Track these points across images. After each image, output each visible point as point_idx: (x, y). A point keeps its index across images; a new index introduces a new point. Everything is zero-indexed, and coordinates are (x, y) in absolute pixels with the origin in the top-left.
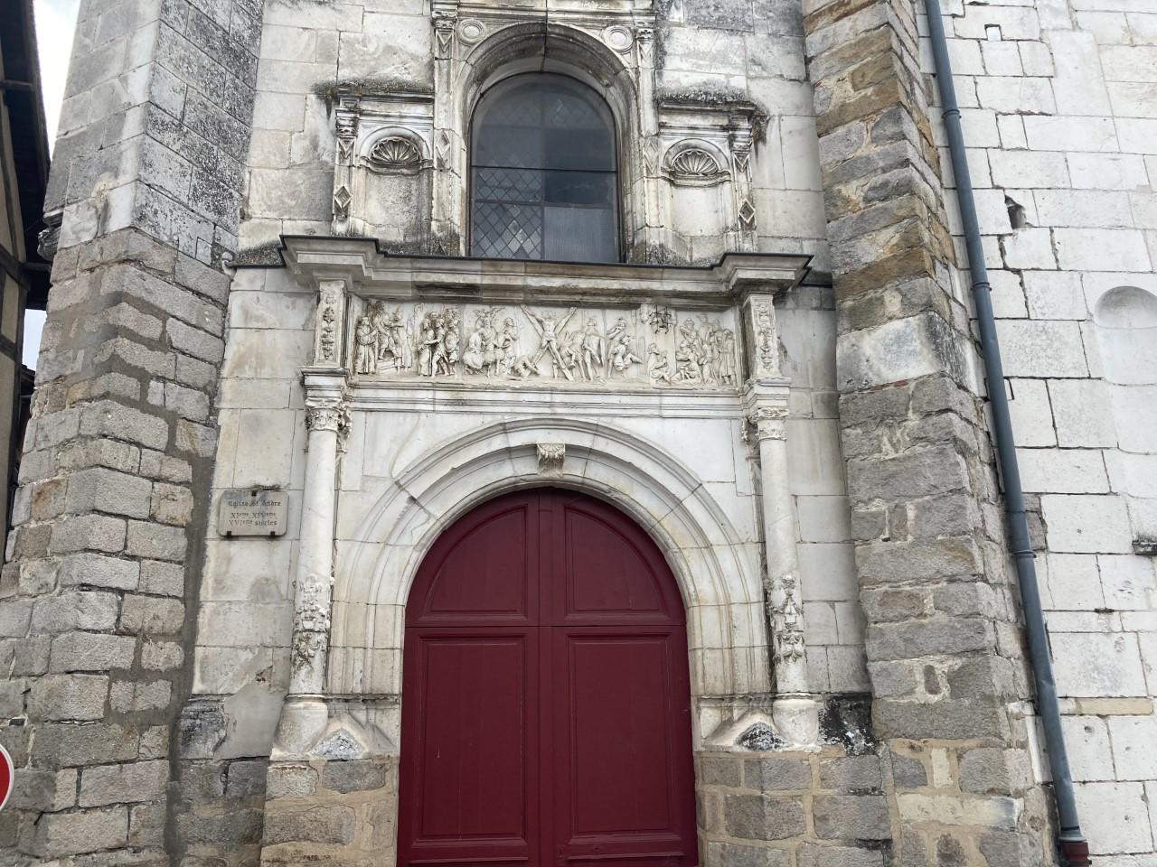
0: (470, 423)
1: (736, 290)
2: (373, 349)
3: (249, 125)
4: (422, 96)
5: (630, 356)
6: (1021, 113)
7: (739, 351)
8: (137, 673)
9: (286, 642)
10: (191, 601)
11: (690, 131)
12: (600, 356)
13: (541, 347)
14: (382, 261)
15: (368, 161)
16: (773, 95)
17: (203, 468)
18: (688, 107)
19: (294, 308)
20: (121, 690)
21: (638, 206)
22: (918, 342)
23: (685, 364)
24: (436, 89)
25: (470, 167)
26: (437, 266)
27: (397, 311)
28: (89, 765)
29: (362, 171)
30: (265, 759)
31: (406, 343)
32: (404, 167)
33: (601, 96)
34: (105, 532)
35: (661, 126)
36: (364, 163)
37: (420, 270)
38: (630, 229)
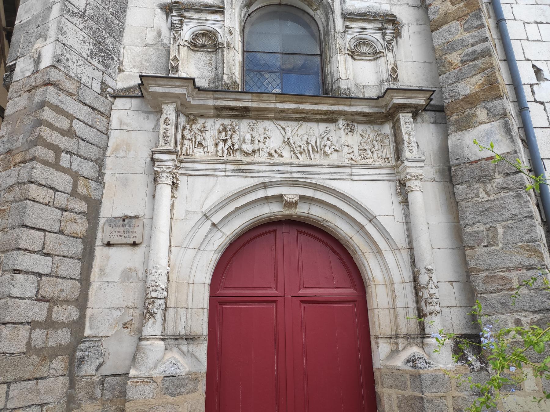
1: (391, 111)
2: (192, 142)
3: (123, 23)
4: (219, 10)
5: (333, 147)
6: (537, 23)
7: (393, 145)
9: (140, 305)
11: (362, 30)
12: (317, 147)
13: (284, 142)
14: (196, 94)
15: (188, 43)
18: (361, 17)
19: (148, 119)
20: (38, 335)
21: (334, 69)
23: (363, 151)
24: (225, 6)
25: (243, 51)
26: (227, 97)
27: (205, 122)
28: (15, 381)
29: (185, 48)
30: (126, 374)
31: (210, 139)
32: (208, 48)
33: (311, 16)
35: (347, 27)
36: (186, 44)
37: (217, 99)
38: (330, 82)
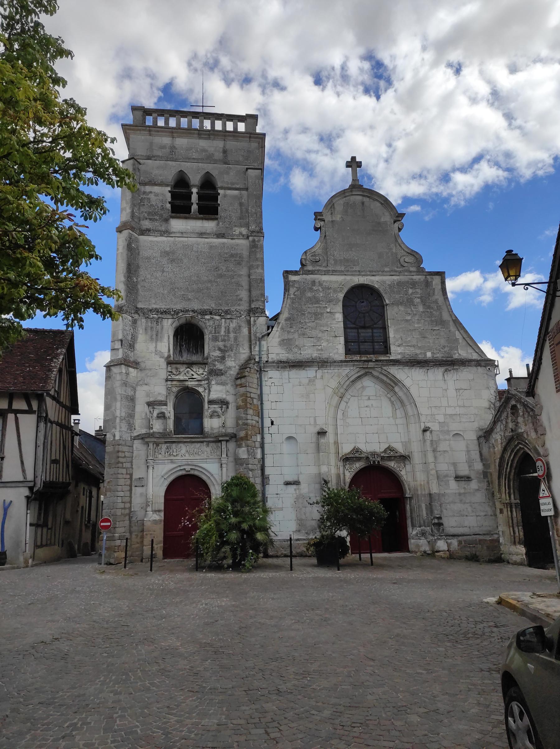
0: (175, 466)
4: (166, 405)
8: (125, 508)
10: (131, 497)
16: (230, 398)
17: (131, 475)
20: (123, 511)
22: (246, 452)
30: (144, 520)
34: (119, 488)
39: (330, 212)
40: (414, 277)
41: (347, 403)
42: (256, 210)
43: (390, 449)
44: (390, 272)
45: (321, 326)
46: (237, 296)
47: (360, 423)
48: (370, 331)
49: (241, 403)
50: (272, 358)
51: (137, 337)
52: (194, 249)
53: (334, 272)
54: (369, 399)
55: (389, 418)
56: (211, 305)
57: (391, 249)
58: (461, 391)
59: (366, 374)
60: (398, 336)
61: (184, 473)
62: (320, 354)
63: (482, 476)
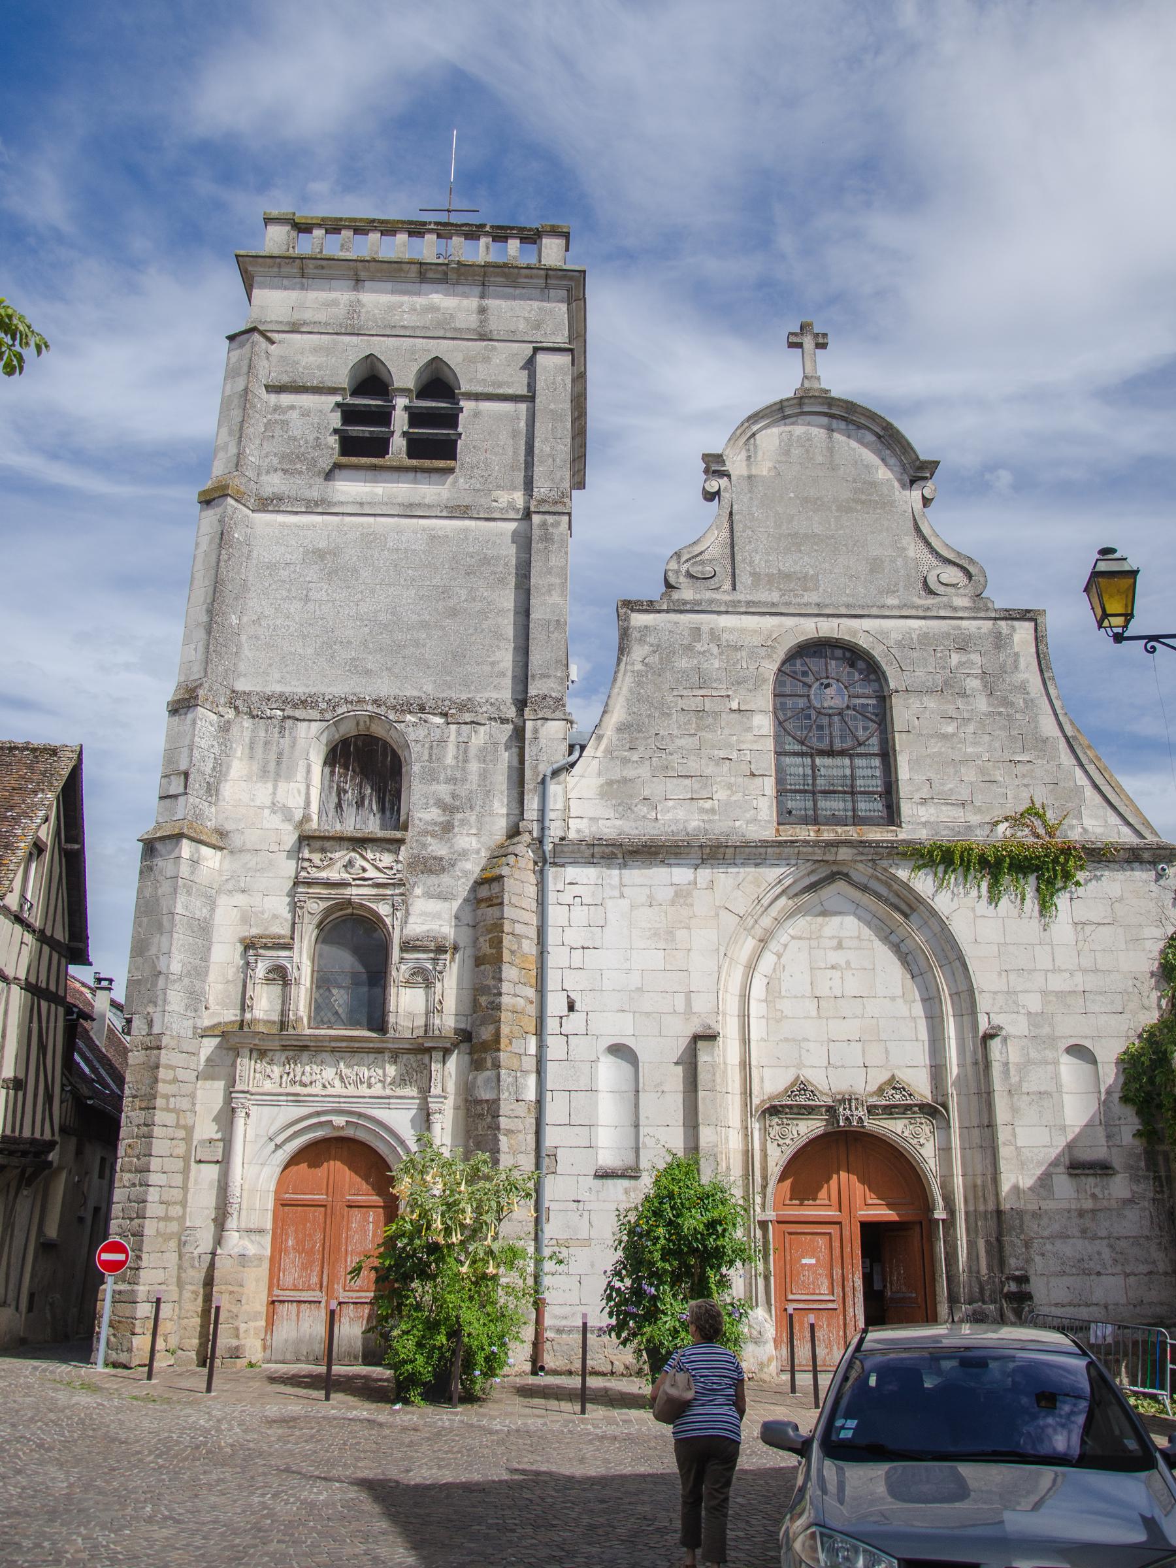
4: (288, 947)
6: (583, 948)
8: (167, 1218)
10: (185, 1188)
17: (190, 1130)
20: (162, 1224)
39: (744, 454)
40: (965, 623)
41: (779, 956)
42: (552, 448)
43: (893, 1084)
44: (900, 607)
45: (713, 747)
46: (493, 664)
47: (814, 1013)
48: (847, 761)
49: (486, 949)
50: (578, 831)
51: (229, 767)
52: (390, 544)
53: (752, 609)
54: (840, 946)
55: (893, 999)
56: (425, 687)
57: (904, 549)
58: (1088, 929)
59: (831, 878)
60: (920, 777)
61: (319, 1134)
62: (710, 821)
63: (1142, 1164)
